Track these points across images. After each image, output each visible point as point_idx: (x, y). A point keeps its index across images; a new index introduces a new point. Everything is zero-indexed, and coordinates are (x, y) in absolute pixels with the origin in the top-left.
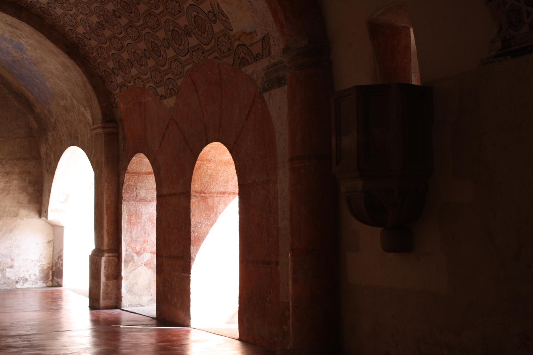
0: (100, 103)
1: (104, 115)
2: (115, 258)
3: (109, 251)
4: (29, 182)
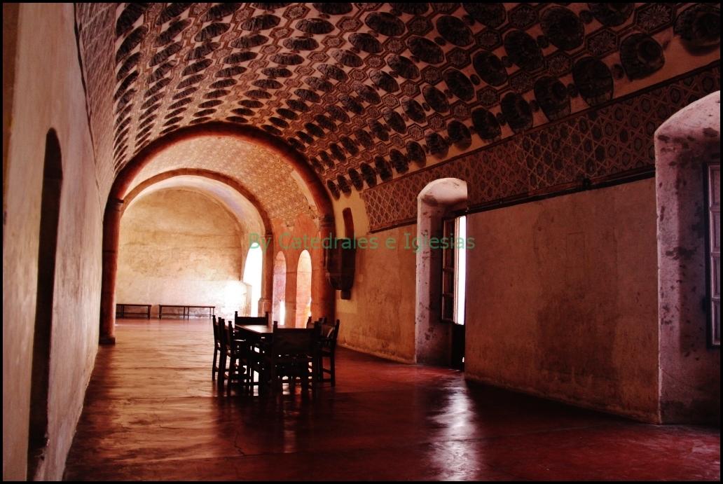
1: (267, 231)
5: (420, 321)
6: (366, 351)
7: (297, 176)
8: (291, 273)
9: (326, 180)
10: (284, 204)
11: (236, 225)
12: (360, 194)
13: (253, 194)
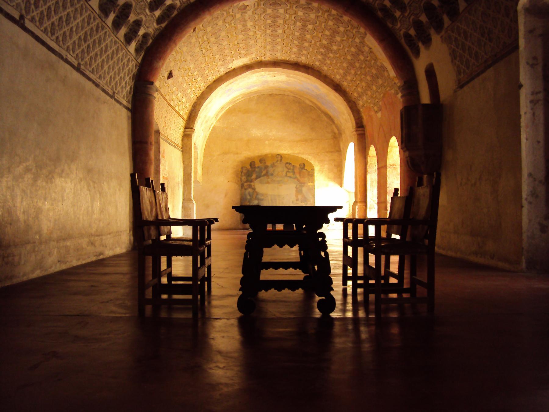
0: (354, 117)
1: (357, 124)
2: (363, 206)
3: (361, 202)
4: (335, 166)
5: (530, 203)
6: (459, 255)
7: (371, 42)
8: (382, 167)
9: (402, 33)
10: (369, 87)
11: (334, 127)
12: (441, 37)
13: (338, 82)
